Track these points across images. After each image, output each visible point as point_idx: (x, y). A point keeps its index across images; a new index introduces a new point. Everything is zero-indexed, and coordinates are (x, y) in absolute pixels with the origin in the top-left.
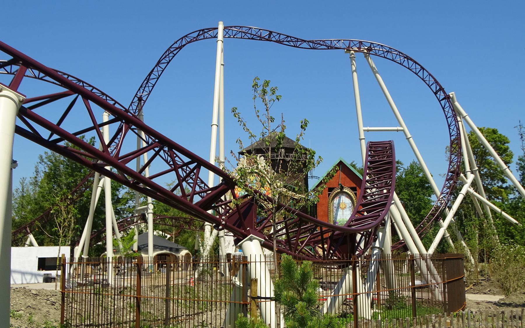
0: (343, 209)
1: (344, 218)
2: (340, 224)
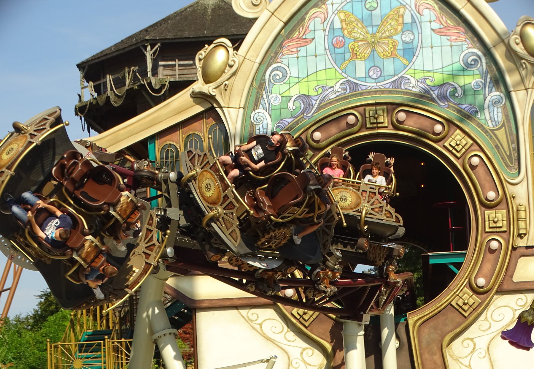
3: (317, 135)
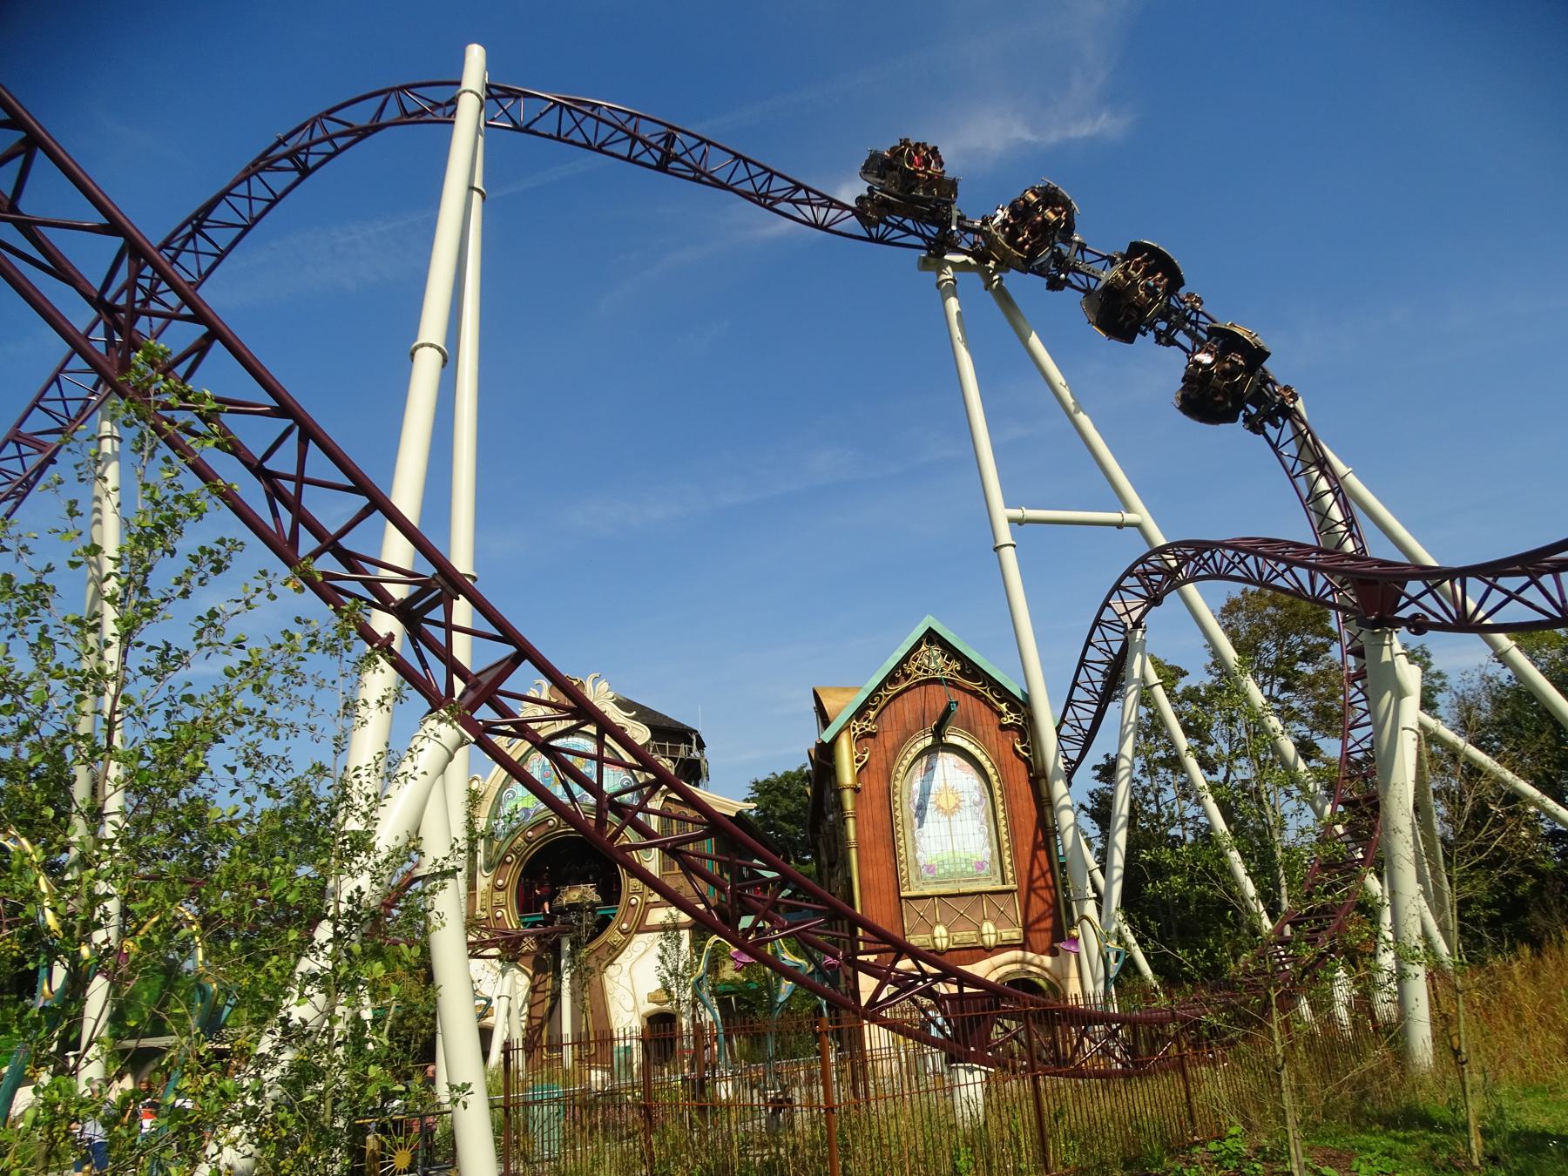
0: (949, 813)
1: (956, 847)
2: (941, 871)
3: (530, 834)
